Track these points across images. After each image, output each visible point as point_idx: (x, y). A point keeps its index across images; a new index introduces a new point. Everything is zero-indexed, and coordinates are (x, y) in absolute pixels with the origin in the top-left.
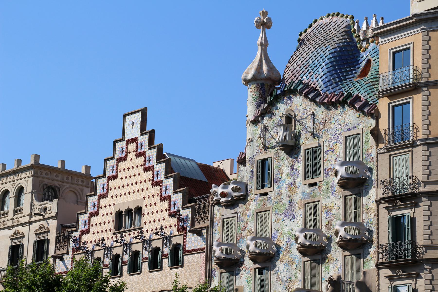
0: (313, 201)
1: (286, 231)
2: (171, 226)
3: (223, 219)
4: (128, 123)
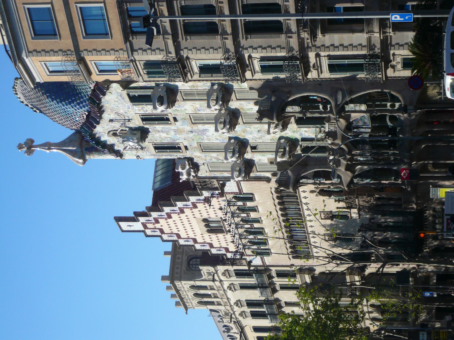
2: (219, 202)
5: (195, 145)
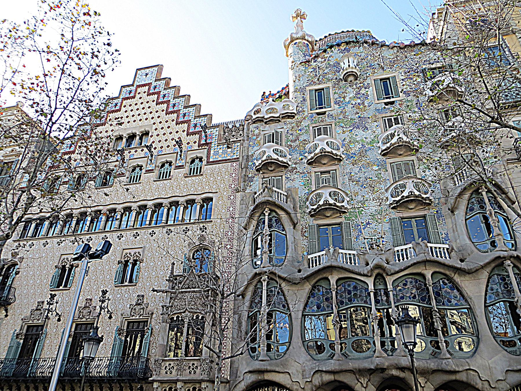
3: (264, 134)
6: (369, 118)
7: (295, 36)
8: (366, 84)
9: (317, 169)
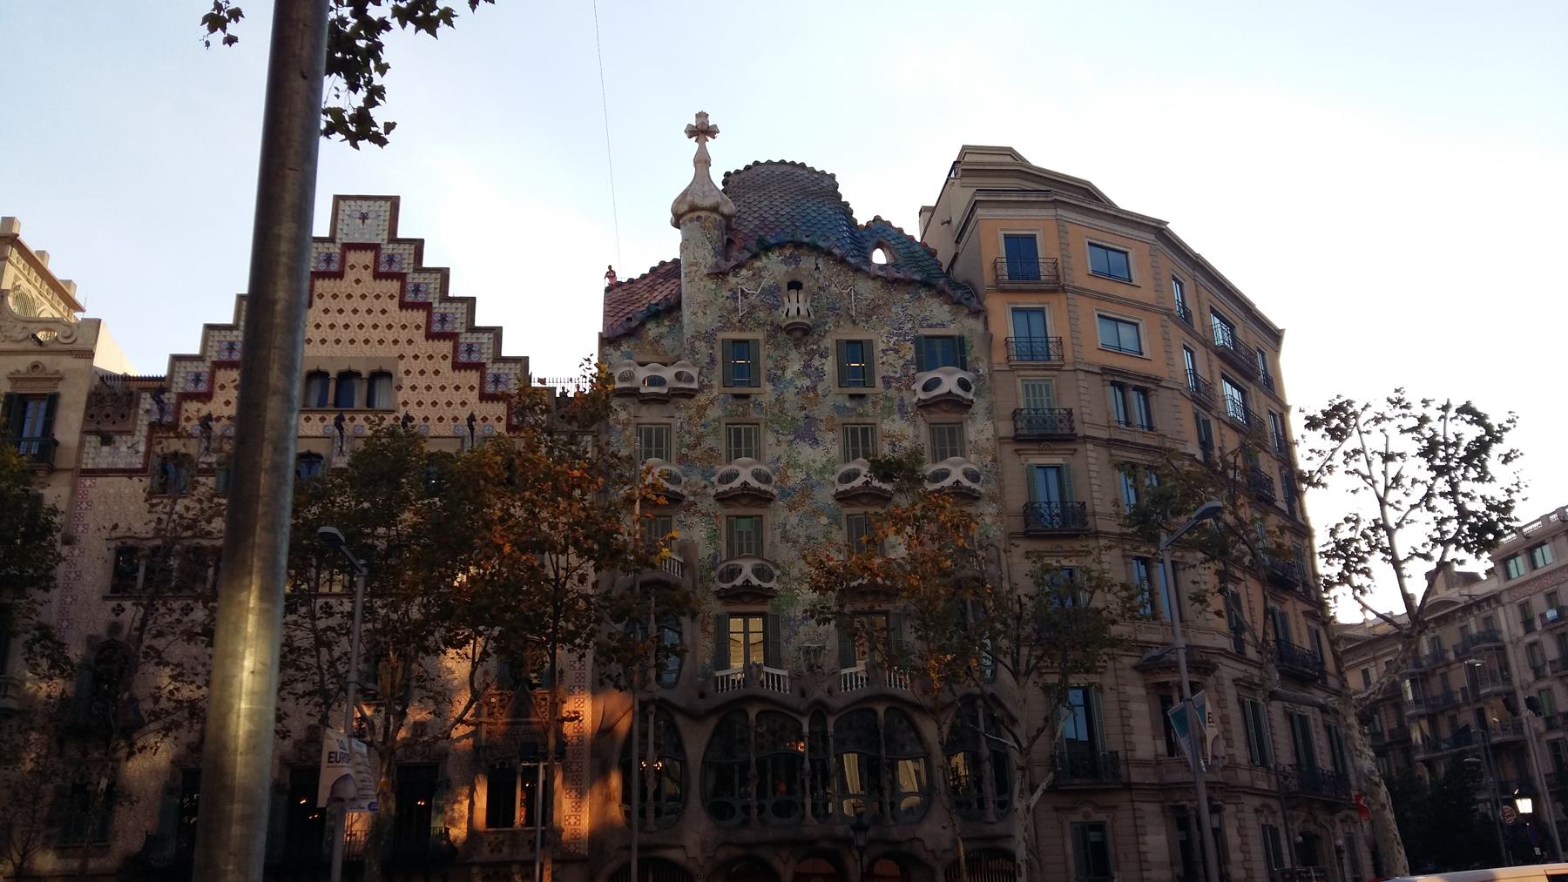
0: (860, 420)
1: (802, 462)
4: (347, 212)
5: (754, 415)
6: (821, 421)
7: (700, 202)
8: (822, 346)
9: (731, 511)
